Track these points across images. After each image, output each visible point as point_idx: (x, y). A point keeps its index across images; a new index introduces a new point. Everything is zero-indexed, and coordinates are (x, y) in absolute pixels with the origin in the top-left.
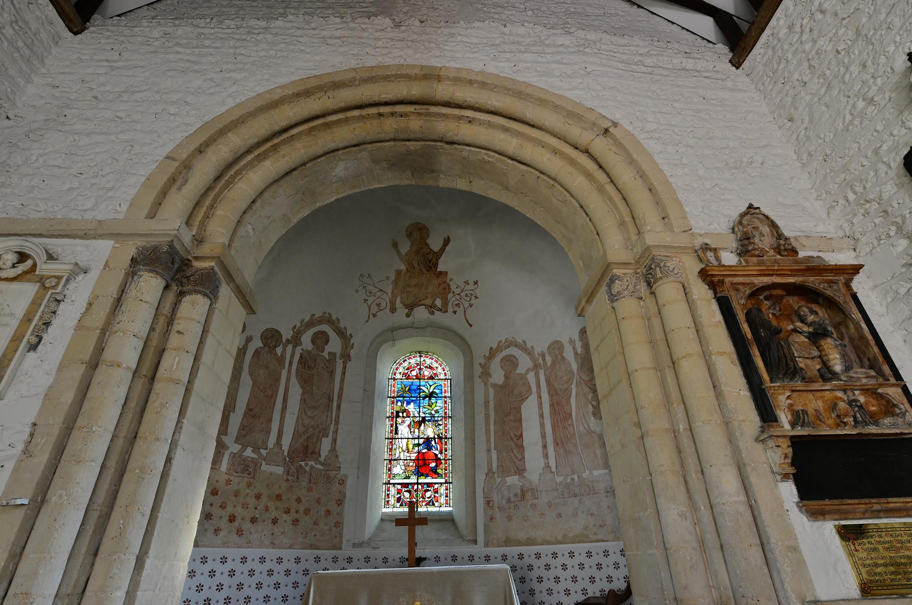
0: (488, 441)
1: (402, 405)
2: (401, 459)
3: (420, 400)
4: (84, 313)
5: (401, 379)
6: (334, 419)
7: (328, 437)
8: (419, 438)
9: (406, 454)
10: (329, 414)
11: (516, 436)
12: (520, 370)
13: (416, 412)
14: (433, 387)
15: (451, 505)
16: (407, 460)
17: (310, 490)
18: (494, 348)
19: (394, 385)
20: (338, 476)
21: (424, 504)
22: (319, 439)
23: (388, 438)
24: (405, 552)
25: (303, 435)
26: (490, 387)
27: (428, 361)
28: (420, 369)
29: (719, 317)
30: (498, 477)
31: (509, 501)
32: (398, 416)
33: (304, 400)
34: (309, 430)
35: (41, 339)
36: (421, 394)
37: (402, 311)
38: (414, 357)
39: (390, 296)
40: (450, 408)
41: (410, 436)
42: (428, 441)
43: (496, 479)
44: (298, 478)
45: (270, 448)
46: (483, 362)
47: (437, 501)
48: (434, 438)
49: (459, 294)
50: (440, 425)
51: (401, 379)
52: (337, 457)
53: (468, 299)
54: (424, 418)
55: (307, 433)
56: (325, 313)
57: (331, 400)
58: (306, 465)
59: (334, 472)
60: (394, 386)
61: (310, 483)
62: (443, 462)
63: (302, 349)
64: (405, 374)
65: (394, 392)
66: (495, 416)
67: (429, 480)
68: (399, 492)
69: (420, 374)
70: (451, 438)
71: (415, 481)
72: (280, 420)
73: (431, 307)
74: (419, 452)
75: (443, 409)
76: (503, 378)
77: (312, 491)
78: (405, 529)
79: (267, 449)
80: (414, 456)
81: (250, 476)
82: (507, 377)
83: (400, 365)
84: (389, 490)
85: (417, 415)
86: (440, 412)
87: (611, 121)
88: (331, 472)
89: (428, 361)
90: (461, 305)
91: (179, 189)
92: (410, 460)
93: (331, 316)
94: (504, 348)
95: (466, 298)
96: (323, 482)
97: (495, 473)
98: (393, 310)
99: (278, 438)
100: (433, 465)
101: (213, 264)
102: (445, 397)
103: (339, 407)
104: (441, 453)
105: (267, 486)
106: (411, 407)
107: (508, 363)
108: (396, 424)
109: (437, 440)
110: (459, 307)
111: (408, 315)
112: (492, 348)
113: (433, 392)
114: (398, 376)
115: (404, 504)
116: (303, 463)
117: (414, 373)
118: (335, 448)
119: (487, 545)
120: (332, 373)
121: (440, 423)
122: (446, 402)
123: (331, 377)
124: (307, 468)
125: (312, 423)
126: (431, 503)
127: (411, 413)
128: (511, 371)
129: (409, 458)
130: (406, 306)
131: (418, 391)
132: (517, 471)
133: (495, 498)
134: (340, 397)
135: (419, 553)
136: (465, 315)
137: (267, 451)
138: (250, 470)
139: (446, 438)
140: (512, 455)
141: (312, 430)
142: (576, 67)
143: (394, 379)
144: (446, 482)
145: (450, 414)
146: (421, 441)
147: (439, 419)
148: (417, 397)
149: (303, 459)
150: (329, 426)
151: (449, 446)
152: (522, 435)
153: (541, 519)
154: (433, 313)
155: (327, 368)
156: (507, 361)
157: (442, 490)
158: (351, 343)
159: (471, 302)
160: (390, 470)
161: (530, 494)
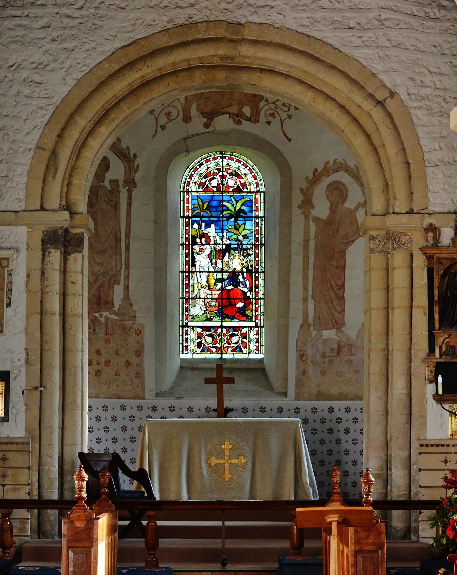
0: (305, 288)
1: (200, 228)
2: (200, 298)
3: (223, 221)
4: (27, 281)
5: (198, 192)
6: (123, 263)
7: (119, 284)
8: (222, 271)
9: (206, 291)
10: (118, 257)
11: (337, 285)
12: (349, 204)
13: (218, 238)
14: (240, 203)
15: (263, 352)
16: (207, 298)
17: (107, 341)
18: (320, 169)
19: (188, 199)
20: (135, 326)
21: (230, 350)
22: (111, 287)
23: (183, 272)
24: (213, 403)
25: (94, 285)
26: (311, 222)
27: (234, 165)
28: (223, 177)
29: (426, 281)
30: (314, 330)
31: (324, 356)
32: (194, 243)
35: (10, 299)
36: (225, 213)
38: (214, 159)
39: (183, 104)
40: (263, 233)
41: (212, 269)
42: (233, 276)
43: (311, 332)
44: (94, 330)
46: (304, 186)
47: (245, 347)
48: (242, 272)
49: (274, 103)
50: (250, 255)
51: (198, 192)
52: (131, 305)
53: (286, 109)
54: (228, 246)
55: (98, 282)
57: (119, 240)
58: (101, 316)
59: (130, 322)
60: (188, 202)
61: (107, 334)
62: (253, 301)
64: (202, 185)
65: (188, 210)
66: (315, 258)
67: (235, 323)
68: (199, 336)
69: (223, 185)
70: (264, 272)
71: (219, 324)
73: (237, 115)
74: (222, 289)
75: (254, 233)
76: (329, 212)
77: (110, 343)
78: (214, 387)
80: (216, 294)
82: (333, 211)
83: (194, 171)
84: (187, 334)
85: (219, 241)
86: (250, 238)
87: (390, 90)
88: (127, 322)
89: (234, 165)
90: (276, 114)
91: (54, 177)
92: (212, 299)
94: (331, 172)
95: (283, 108)
96: (119, 332)
97: (310, 325)
98: (187, 119)
100: (241, 305)
101: (83, 230)
102: (257, 217)
103: (128, 248)
104: (251, 290)
106: (212, 231)
107: (336, 192)
108: (193, 253)
109: (245, 274)
110: (274, 117)
111: (207, 126)
112: (316, 170)
113: (240, 211)
114: (193, 188)
115: (206, 350)
116: (97, 315)
117: (214, 183)
119: (297, 398)
120: (116, 206)
121: (250, 252)
122: (257, 224)
123: (116, 211)
124: (102, 320)
125: (101, 270)
126: (238, 349)
127: (212, 238)
128: (338, 203)
129: (210, 296)
130: (203, 114)
131: (220, 209)
132: (335, 325)
133: (309, 352)
134: (128, 236)
135: (227, 404)
136: (282, 127)
139: (257, 271)
140: (330, 305)
142: (371, 15)
143: (188, 192)
144: (257, 326)
145: (262, 240)
146: (225, 276)
147: (249, 247)
148: (219, 217)
149: (97, 310)
150: (119, 271)
151: (261, 282)
152: (344, 284)
153: (356, 376)
154: (239, 123)
155: (110, 201)
156: (335, 189)
157: (252, 335)
158: (136, 165)
159: (289, 113)
160: (187, 310)
161: (346, 349)
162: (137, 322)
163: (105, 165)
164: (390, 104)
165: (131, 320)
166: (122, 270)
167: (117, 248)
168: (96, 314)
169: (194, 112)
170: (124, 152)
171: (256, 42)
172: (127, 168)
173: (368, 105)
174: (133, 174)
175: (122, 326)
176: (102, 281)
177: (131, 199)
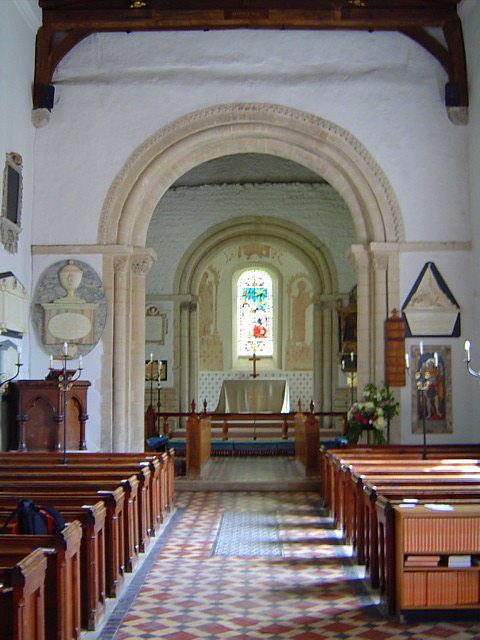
37: (244, 257)
78: (252, 362)
119: (286, 370)
120: (211, 292)
130: (246, 254)
164: (322, 249)
169: (242, 253)
171: (267, 224)
173: (313, 249)
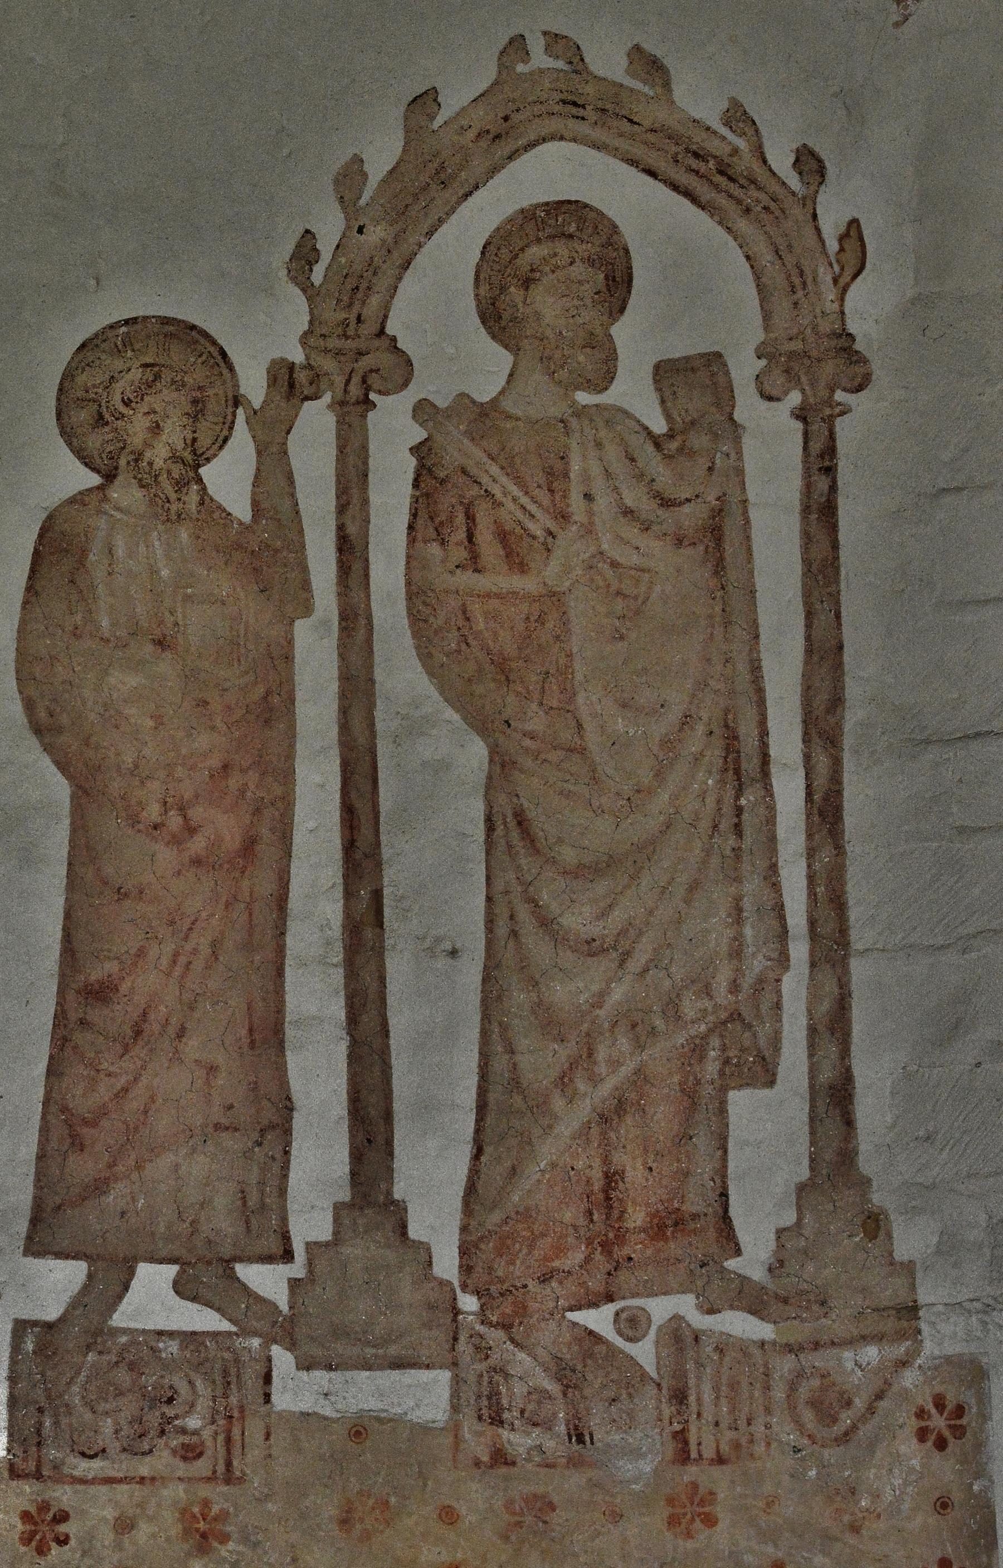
6: (797, 917)
10: (752, 886)
20: (909, 1378)
25: (558, 1103)
33: (521, 820)
34: (602, 1053)
44: (578, 1435)
45: (310, 1247)
56: (517, 45)
57: (750, 766)
59: (871, 1353)
61: (683, 1456)
63: (423, 410)
72: (353, 1020)
77: (710, 1521)
79: (288, 1256)
81: (202, 1467)
93: (576, 57)
99: (357, 1157)
105: (345, 1522)
118: (847, 1157)
123: (719, 568)
125: (618, 994)
137: (297, 1269)
138: (193, 1422)
141: (624, 1043)
149: (596, 1283)
155: (667, 503)
158: (831, 226)
162: (929, 1348)
163: (590, 262)
165: (878, 1338)
166: (786, 979)
167: (738, 829)
168: (583, 1317)
170: (714, 146)
172: (766, 255)
174: (830, 294)
175: (804, 1392)
176: (626, 1070)
177: (830, 471)
